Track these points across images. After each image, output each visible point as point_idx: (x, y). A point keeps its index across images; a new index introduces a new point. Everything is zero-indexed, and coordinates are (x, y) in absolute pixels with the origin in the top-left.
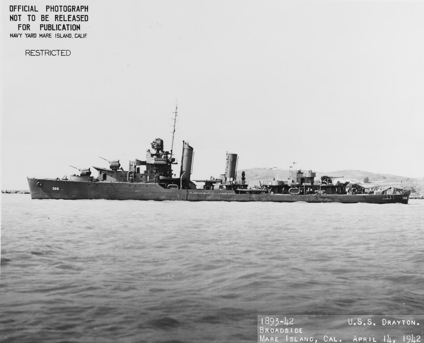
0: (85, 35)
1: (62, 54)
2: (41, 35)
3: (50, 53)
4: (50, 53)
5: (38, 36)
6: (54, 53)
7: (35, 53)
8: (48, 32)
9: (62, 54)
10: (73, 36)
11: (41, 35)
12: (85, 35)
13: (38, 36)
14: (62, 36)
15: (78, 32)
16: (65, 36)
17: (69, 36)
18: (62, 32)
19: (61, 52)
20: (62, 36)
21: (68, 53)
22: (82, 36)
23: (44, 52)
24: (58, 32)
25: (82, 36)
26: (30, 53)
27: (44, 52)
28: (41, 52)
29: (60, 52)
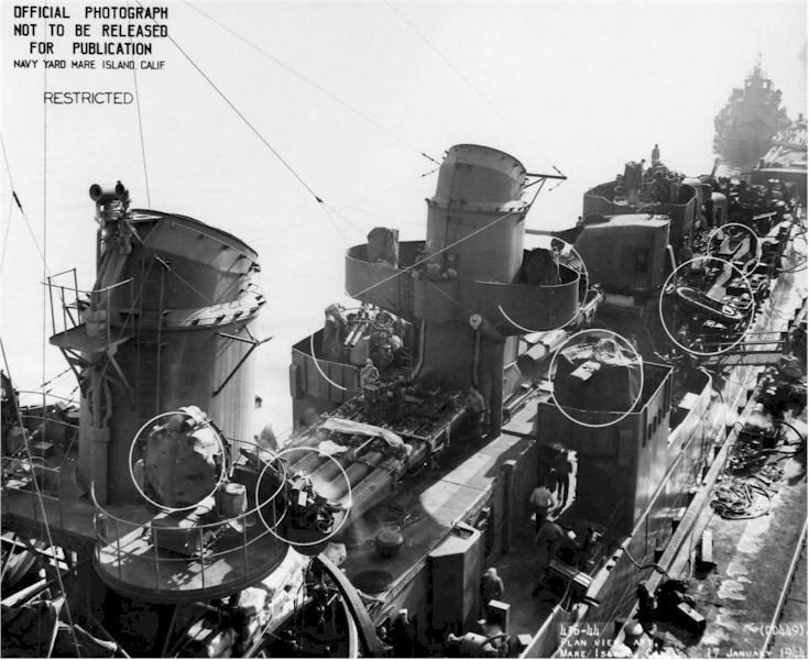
0: (161, 64)
1: (117, 101)
2: (75, 64)
3: (93, 98)
4: (93, 98)
5: (69, 64)
6: (99, 98)
7: (61, 98)
8: (88, 57)
9: (117, 101)
10: (137, 65)
11: (75, 64)
12: (161, 64)
13: (69, 64)
14: (116, 65)
15: (147, 57)
16: (120, 65)
17: (130, 65)
18: (117, 59)
19: (115, 97)
20: (116, 65)
21: (128, 98)
22: (156, 66)
23: (80, 96)
24: (108, 57)
25: (156, 66)
26: (52, 98)
27: (80, 96)
28: (74, 96)
29: (112, 96)
